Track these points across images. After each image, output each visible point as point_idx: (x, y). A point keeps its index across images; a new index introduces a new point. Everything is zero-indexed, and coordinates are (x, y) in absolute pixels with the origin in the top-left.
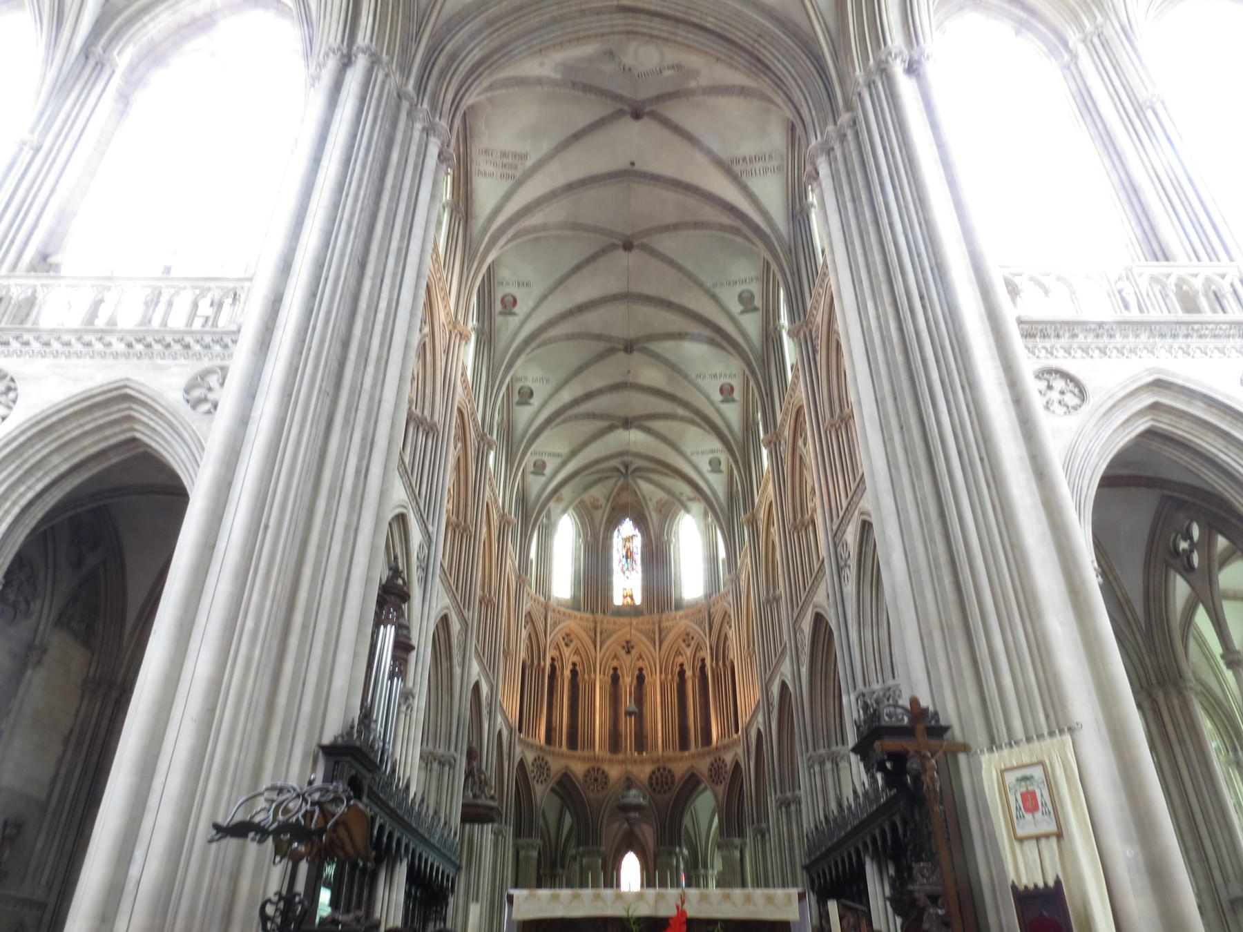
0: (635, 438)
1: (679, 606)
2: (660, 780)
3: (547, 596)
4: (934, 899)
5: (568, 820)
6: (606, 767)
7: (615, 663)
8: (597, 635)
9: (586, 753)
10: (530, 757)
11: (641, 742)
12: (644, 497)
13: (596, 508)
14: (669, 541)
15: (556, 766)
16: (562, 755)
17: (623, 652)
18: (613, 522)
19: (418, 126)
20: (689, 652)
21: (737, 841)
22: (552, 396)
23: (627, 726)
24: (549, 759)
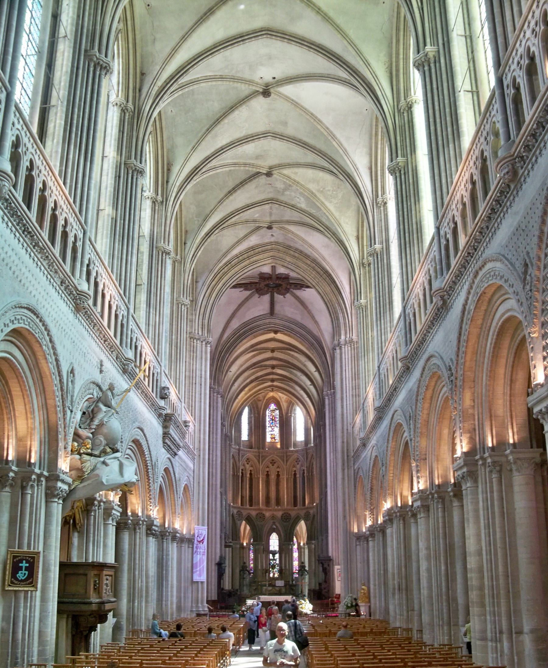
0: (275, 383)
1: (295, 445)
2: (286, 517)
3: (239, 445)
4: (325, 589)
5: (248, 528)
6: (264, 512)
7: (267, 469)
8: (260, 457)
9: (256, 508)
10: (235, 511)
11: (278, 502)
12: (280, 397)
13: (260, 400)
14: (291, 416)
15: (245, 513)
16: (247, 509)
17: (271, 465)
18: (267, 406)
19: (215, 394)
20: (298, 466)
21: (313, 542)
22: (242, 383)
23: (273, 495)
24: (242, 511)
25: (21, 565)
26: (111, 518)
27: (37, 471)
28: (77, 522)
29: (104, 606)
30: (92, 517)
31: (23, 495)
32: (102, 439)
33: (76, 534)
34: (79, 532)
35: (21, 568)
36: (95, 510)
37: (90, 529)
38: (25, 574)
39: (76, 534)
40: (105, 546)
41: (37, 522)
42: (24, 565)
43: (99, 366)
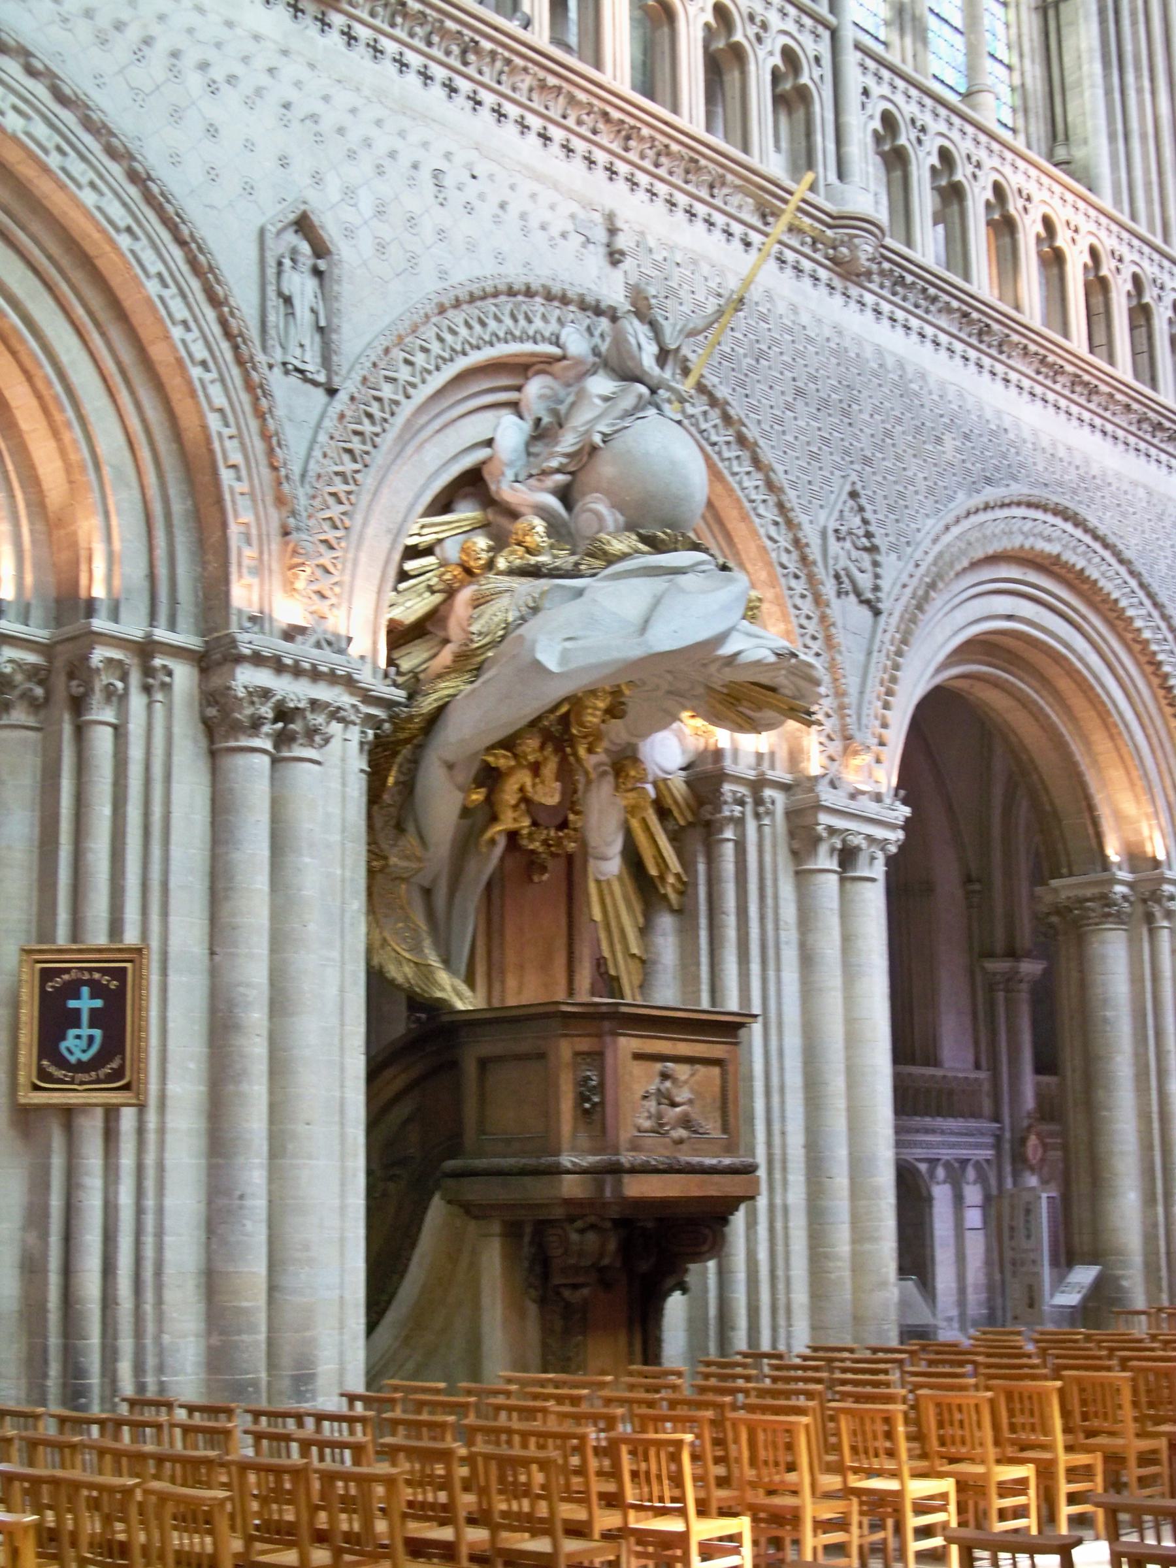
25: (72, 1004)
26: (823, 849)
27: (133, 627)
28: (653, 872)
29: (618, 1184)
30: (729, 850)
31: (80, 732)
32: (602, 508)
33: (666, 922)
34: (678, 912)
35: (73, 1018)
36: (740, 822)
37: (721, 896)
38: (91, 1038)
39: (666, 922)
40: (807, 959)
41: (157, 832)
42: (85, 1003)
43: (601, 235)
